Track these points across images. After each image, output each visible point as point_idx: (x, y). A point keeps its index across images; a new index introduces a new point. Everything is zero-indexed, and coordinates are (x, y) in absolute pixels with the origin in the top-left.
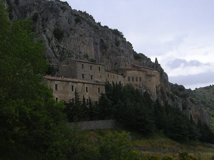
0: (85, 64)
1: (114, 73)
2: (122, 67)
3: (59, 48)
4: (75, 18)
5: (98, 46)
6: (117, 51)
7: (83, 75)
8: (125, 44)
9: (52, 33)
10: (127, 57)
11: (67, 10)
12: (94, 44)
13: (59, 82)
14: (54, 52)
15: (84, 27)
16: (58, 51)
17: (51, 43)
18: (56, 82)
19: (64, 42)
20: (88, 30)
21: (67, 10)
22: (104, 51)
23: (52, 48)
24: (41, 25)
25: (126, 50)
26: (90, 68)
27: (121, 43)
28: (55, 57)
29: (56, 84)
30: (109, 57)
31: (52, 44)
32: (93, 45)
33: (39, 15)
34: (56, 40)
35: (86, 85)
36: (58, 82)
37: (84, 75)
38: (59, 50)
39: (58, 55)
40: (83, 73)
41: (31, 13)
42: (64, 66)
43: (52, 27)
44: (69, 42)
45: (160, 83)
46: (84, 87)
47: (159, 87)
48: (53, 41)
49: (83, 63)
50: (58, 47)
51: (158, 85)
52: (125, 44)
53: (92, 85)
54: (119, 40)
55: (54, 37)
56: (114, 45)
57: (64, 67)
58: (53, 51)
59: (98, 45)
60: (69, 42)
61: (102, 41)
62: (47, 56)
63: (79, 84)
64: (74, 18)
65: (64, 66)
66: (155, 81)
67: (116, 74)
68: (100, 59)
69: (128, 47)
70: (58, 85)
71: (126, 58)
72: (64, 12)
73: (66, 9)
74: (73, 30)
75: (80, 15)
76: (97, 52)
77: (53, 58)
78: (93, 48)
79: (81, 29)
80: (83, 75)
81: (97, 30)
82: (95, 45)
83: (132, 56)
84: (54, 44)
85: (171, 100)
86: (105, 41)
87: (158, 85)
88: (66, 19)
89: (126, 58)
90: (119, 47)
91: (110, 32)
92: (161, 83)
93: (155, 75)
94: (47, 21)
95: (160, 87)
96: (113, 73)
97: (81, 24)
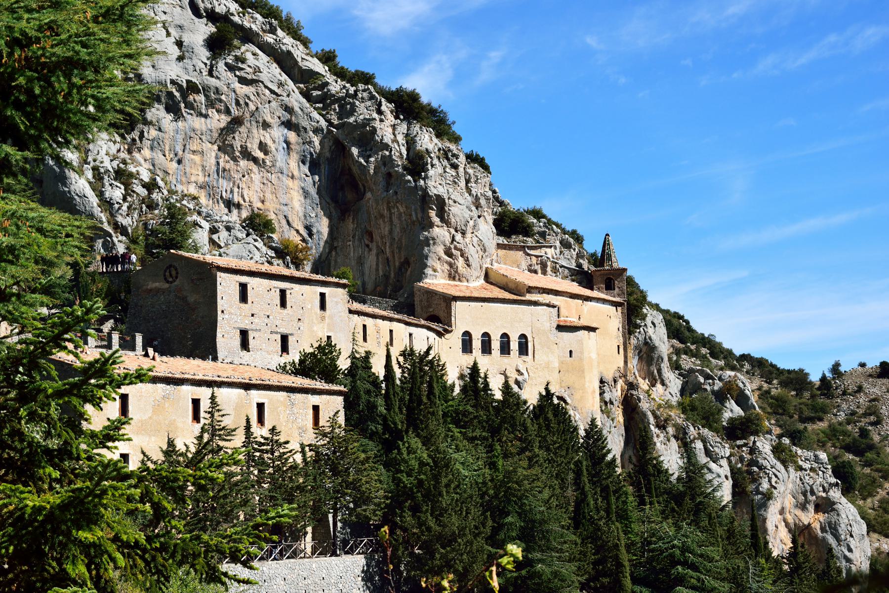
0: (253, 283)
1: (391, 319)
2: (435, 281)
3: (127, 185)
4: (212, 29)
7: (244, 334)
8: (455, 167)
10: (464, 233)
14: (107, 204)
15: (249, 77)
16: (125, 199)
19: (152, 148)
22: (350, 196)
25: (459, 199)
26: (278, 302)
27: (436, 161)
31: (95, 161)
34: (115, 142)
35: (257, 396)
37: (251, 335)
38: (128, 192)
42: (157, 284)
44: (179, 149)
45: (622, 364)
47: (615, 381)
49: (244, 279)
51: (609, 377)
52: (455, 167)
53: (282, 395)
54: (423, 149)
57: (157, 291)
58: (100, 195)
59: (322, 167)
60: (179, 149)
64: (204, 29)
65: (157, 284)
66: (594, 356)
67: (402, 325)
69: (468, 181)
71: (458, 237)
74: (198, 92)
75: (236, 19)
79: (237, 85)
80: (244, 334)
81: (315, 93)
83: (486, 229)
85: (674, 444)
87: (609, 377)
88: (168, 34)
89: (458, 237)
90: (422, 182)
91: (383, 108)
92: (626, 362)
93: (594, 325)
95: (621, 383)
96: (387, 323)
97: (240, 65)
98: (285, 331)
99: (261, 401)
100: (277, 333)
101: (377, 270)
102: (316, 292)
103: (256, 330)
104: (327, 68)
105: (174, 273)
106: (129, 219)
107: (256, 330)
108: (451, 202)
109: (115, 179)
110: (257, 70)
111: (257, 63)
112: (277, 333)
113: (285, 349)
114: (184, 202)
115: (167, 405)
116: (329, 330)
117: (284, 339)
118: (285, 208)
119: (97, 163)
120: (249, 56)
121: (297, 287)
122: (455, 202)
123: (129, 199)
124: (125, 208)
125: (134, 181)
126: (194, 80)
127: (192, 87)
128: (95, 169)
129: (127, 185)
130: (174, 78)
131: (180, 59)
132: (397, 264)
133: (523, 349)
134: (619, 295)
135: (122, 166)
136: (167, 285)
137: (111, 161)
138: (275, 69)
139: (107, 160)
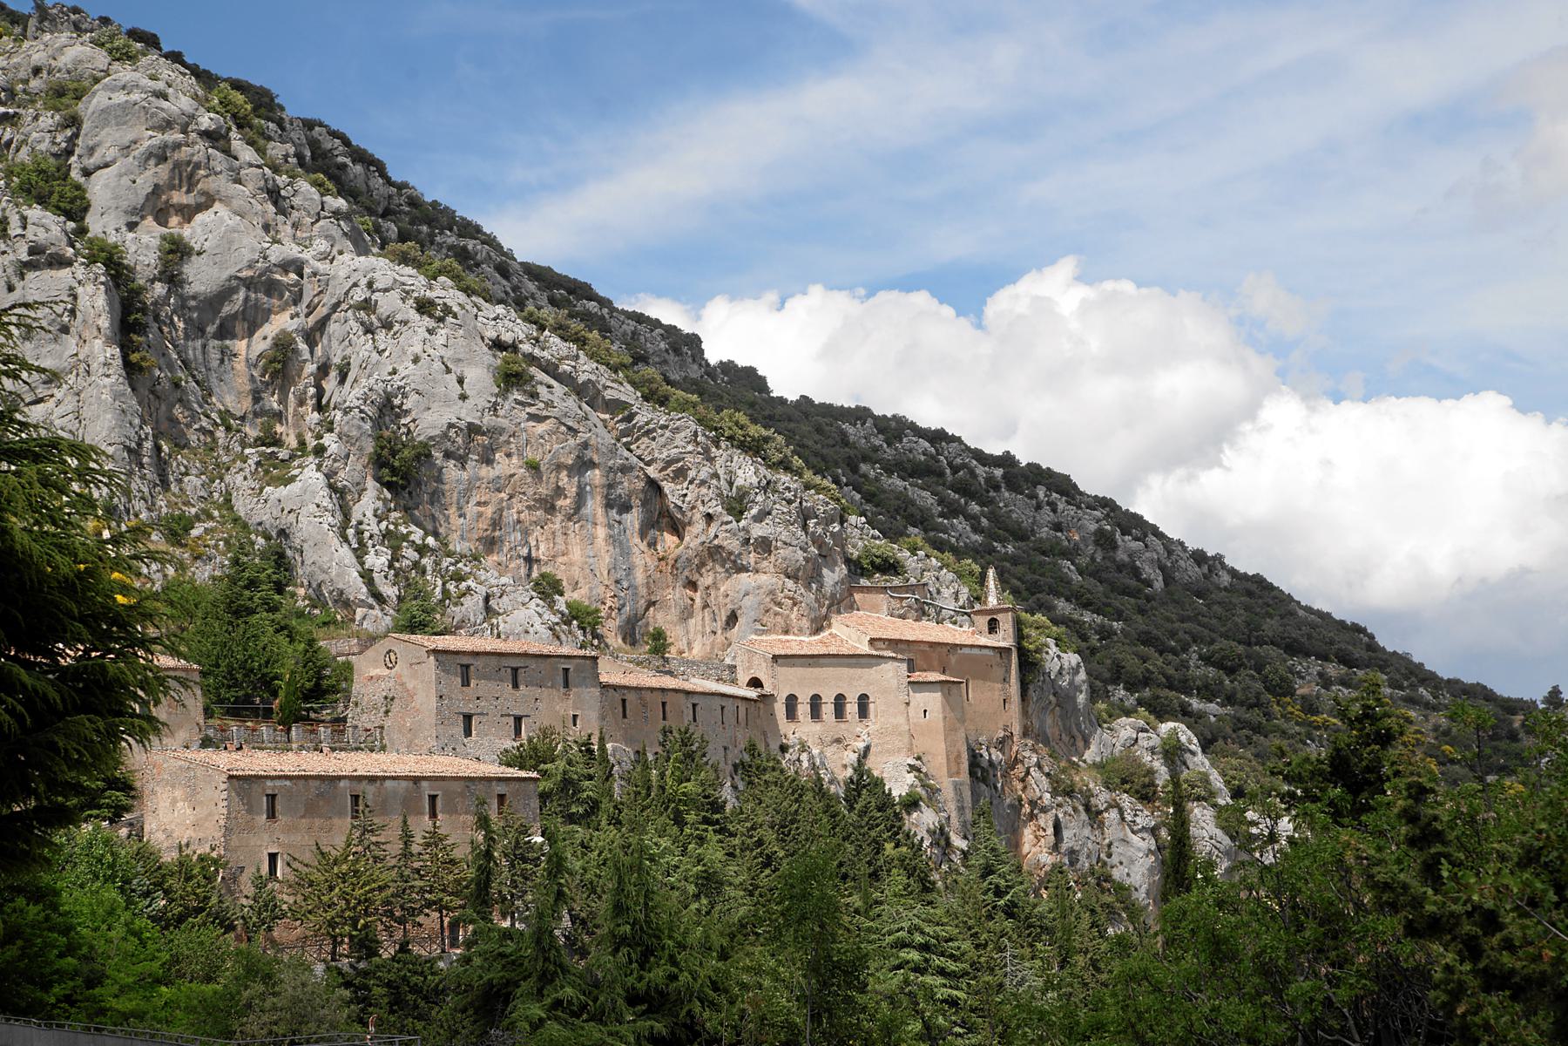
5: (633, 519)
6: (733, 545)
7: (468, 718)
11: (450, 319)
12: (609, 505)
13: (288, 783)
15: (545, 413)
16: (391, 566)
17: (354, 522)
18: (269, 783)
20: (570, 428)
21: (455, 316)
23: (360, 553)
24: (311, 403)
28: (371, 601)
29: (269, 792)
30: (696, 577)
31: (360, 523)
32: (600, 511)
33: (303, 346)
36: (278, 783)
39: (390, 591)
40: (470, 708)
41: (258, 334)
43: (359, 427)
46: (420, 798)
48: (367, 505)
50: (391, 539)
55: (371, 484)
56: (719, 509)
57: (379, 678)
61: (654, 486)
62: (331, 593)
63: (388, 783)
68: (643, 591)
70: (278, 800)
72: (430, 332)
73: (447, 310)
76: (626, 553)
77: (363, 603)
78: (601, 532)
80: (468, 718)
82: (613, 513)
84: (372, 527)
86: (667, 487)
94: (342, 381)
99: (433, 793)
100: (509, 715)
101: (704, 626)
102: (557, 669)
103: (482, 714)
104: (639, 394)
105: (393, 658)
106: (396, 589)
107: (482, 714)
108: (779, 544)
109: (382, 544)
110: (549, 404)
111: (550, 397)
112: (509, 715)
113: (518, 732)
114: (460, 565)
115: (321, 803)
117: (518, 720)
118: (591, 560)
120: (542, 390)
121: (533, 664)
122: (785, 543)
123: (397, 565)
124: (391, 576)
125: (405, 544)
126: (477, 422)
127: (473, 430)
128: (359, 533)
130: (454, 420)
131: (463, 397)
132: (724, 618)
133: (863, 711)
134: (1004, 639)
135: (392, 527)
136: (387, 672)
137: (379, 522)
138: (571, 402)
139: (374, 521)
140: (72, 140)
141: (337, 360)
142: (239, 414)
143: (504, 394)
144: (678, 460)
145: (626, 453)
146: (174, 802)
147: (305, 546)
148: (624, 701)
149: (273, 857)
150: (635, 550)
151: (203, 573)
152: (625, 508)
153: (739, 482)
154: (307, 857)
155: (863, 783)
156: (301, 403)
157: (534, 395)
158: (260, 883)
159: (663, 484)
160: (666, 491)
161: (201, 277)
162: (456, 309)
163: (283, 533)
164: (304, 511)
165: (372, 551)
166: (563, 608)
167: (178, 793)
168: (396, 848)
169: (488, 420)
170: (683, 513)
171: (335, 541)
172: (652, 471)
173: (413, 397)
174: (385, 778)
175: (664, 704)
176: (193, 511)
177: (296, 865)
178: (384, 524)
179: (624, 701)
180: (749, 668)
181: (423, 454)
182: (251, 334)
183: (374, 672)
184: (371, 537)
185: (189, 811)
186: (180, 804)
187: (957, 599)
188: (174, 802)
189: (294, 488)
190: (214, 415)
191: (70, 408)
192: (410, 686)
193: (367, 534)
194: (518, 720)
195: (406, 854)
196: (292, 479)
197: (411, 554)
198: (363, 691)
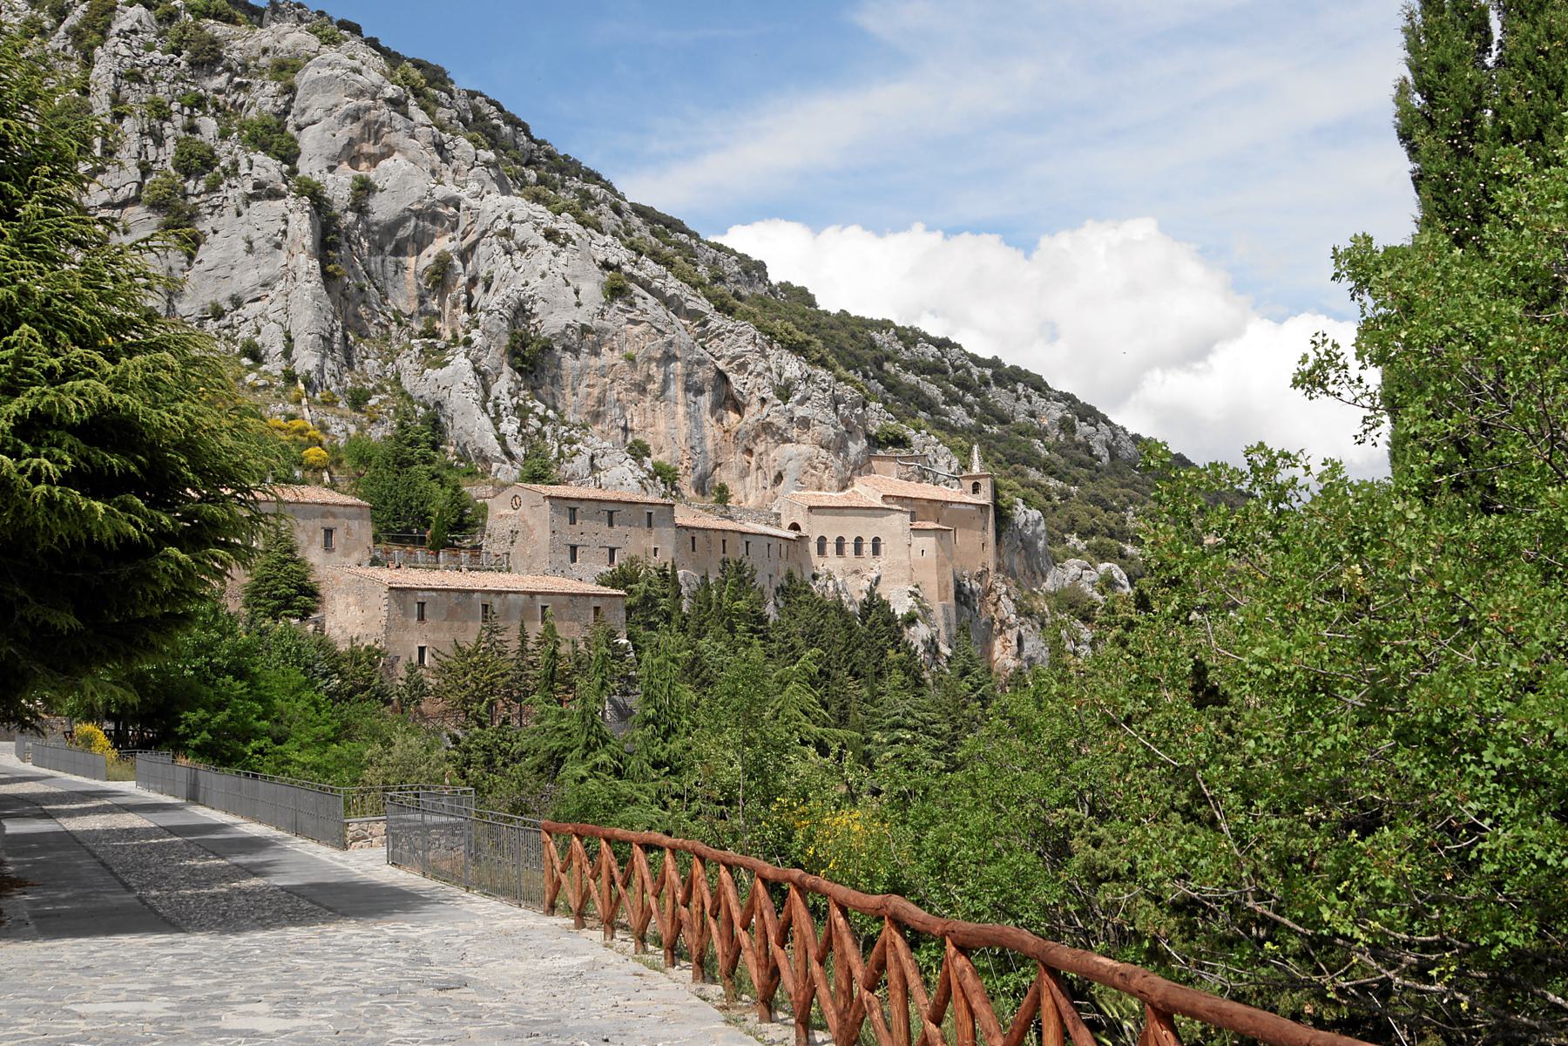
3: (524, 419)
5: (706, 400)
6: (781, 422)
7: (574, 548)
9: (502, 350)
11: (570, 245)
12: (687, 389)
13: (434, 594)
15: (640, 318)
16: (519, 432)
17: (492, 398)
18: (420, 594)
20: (659, 330)
21: (574, 243)
23: (496, 421)
24: (463, 306)
28: (504, 457)
30: (752, 446)
31: (497, 398)
32: (680, 394)
33: (457, 263)
36: (426, 593)
39: (519, 451)
41: (425, 253)
43: (499, 326)
46: (535, 608)
48: (503, 384)
50: (521, 411)
55: (506, 369)
57: (507, 516)
61: (722, 376)
62: (473, 450)
63: (510, 596)
68: (712, 455)
70: (427, 607)
72: (555, 254)
73: (568, 238)
76: (699, 426)
77: (497, 459)
78: (681, 410)
80: (574, 548)
82: (691, 396)
84: (506, 401)
86: (732, 377)
94: (487, 291)
98: (612, 545)
109: (514, 415)
110: (644, 312)
116: (656, 543)
117: (612, 551)
119: (500, 401)
120: (638, 301)
121: (624, 509)
124: (519, 439)
127: (585, 330)
128: (497, 406)
129: (524, 419)
130: (571, 322)
131: (578, 305)
133: (876, 550)
135: (521, 402)
138: (661, 310)
139: (507, 397)
140: (289, 103)
141: (483, 274)
142: (408, 313)
143: (610, 302)
144: (741, 357)
145: (702, 351)
146: (348, 605)
147: (455, 415)
148: (693, 538)
149: (422, 650)
150: (707, 424)
151: (377, 433)
152: (700, 392)
153: (787, 375)
154: (448, 650)
155: (874, 605)
156: (455, 306)
157: (632, 305)
158: (411, 669)
159: (729, 374)
160: (731, 379)
161: (383, 208)
162: (574, 237)
163: (438, 404)
164: (454, 388)
165: (506, 419)
166: (650, 467)
167: (351, 600)
168: (514, 645)
169: (596, 323)
170: (744, 397)
171: (477, 411)
172: (721, 365)
173: (541, 304)
174: (508, 592)
175: (724, 541)
176: (371, 386)
177: (439, 656)
178: (516, 399)
179: (693, 538)
180: (791, 516)
181: (547, 348)
182: (419, 252)
183: (503, 512)
184: (505, 409)
185: (359, 613)
186: (352, 608)
187: (949, 467)
188: (348, 605)
189: (447, 370)
190: (389, 313)
191: (280, 306)
192: (530, 523)
193: (502, 407)
194: (612, 551)
195: (523, 650)
196: (447, 363)
197: (535, 423)
198: (495, 526)
